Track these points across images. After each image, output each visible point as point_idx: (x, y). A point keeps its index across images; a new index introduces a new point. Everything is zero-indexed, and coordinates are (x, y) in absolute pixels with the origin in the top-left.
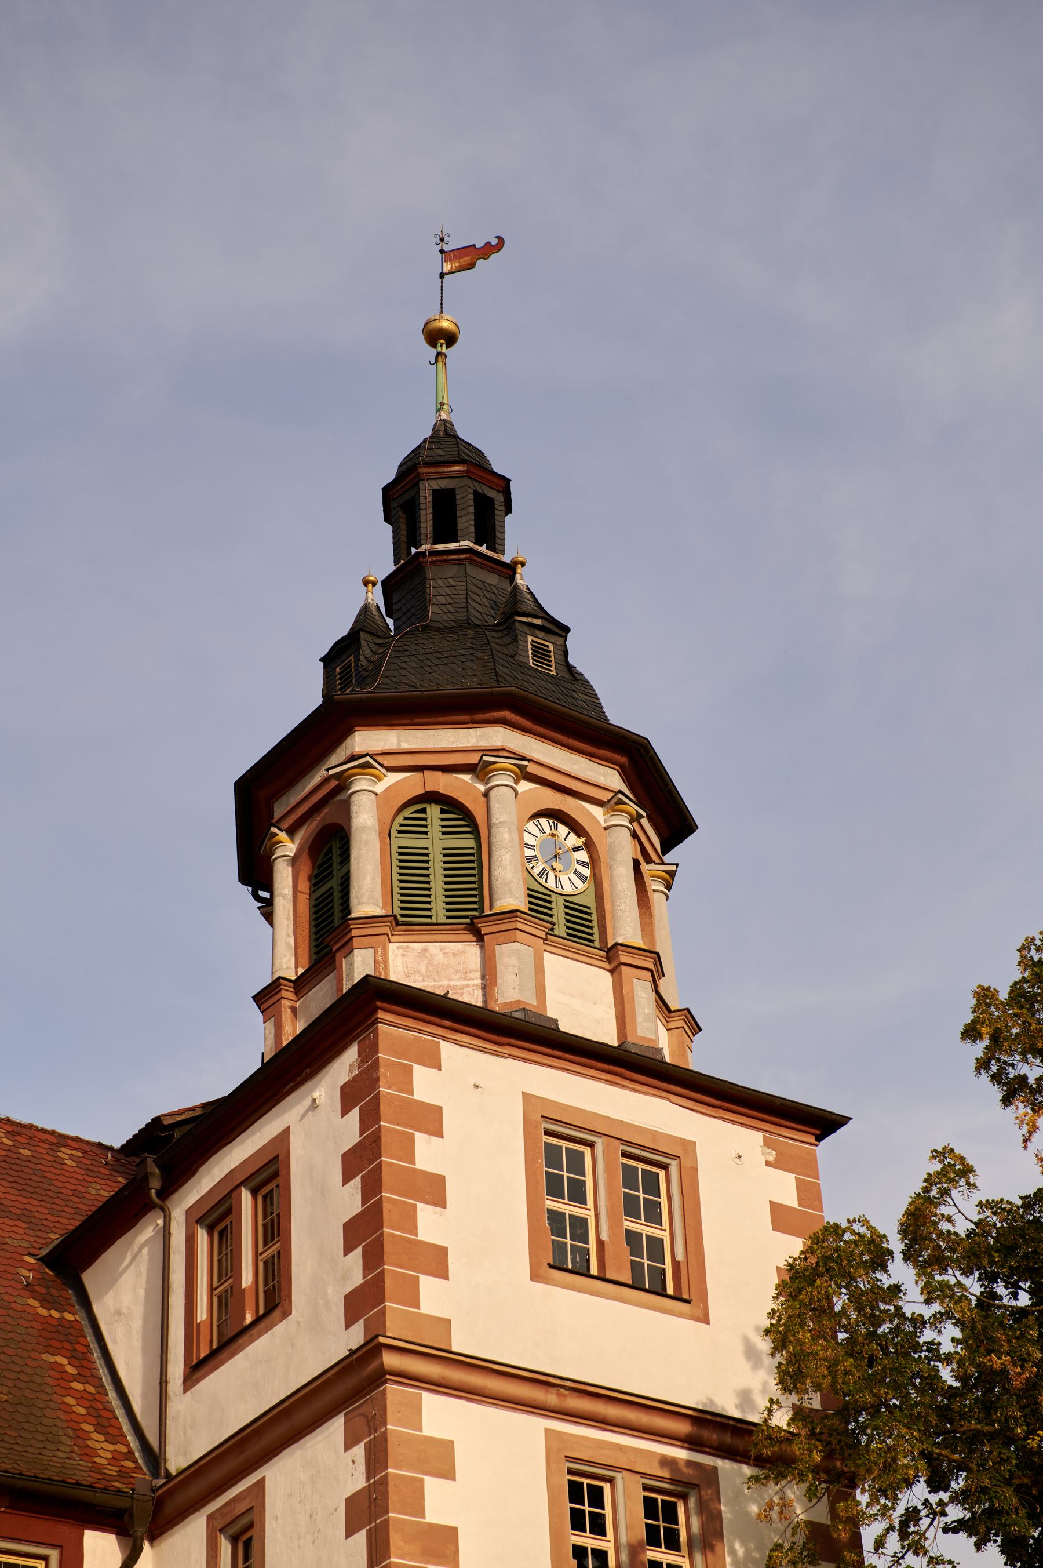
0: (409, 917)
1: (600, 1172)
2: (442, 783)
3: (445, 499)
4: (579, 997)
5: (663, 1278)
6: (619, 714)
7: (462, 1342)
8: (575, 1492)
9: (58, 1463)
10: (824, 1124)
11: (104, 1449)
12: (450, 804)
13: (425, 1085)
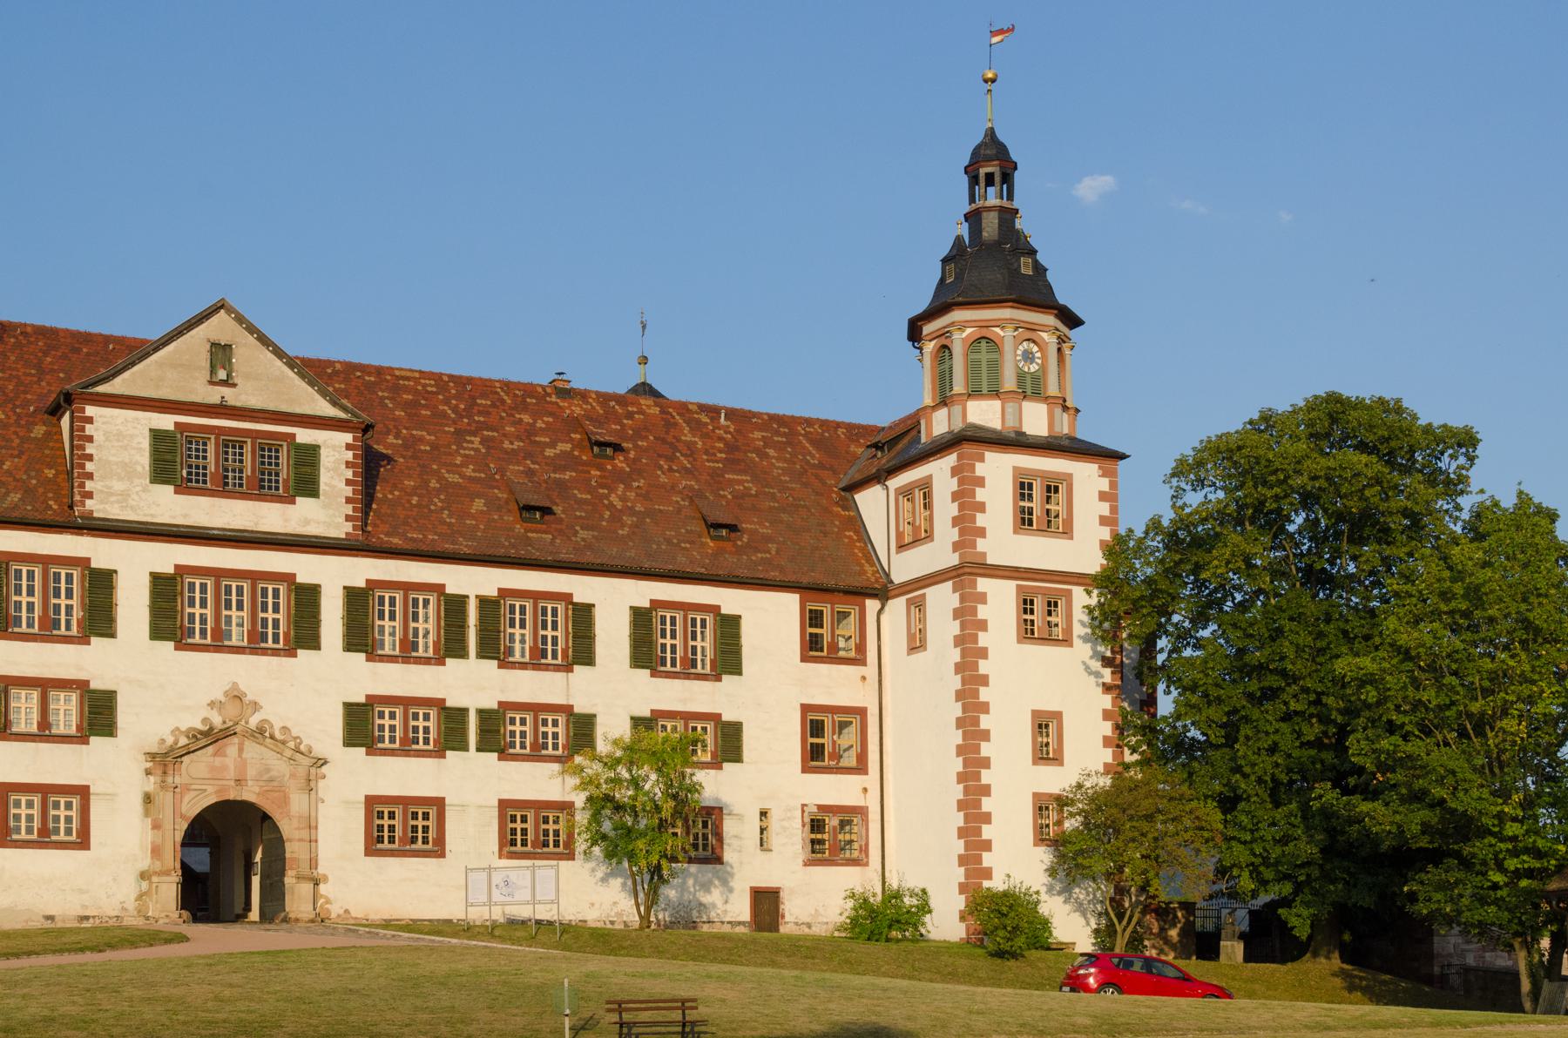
0: (975, 394)
1: (1038, 492)
2: (985, 332)
4: (1036, 420)
8: (1025, 602)
9: (856, 582)
10: (1122, 457)
12: (989, 340)
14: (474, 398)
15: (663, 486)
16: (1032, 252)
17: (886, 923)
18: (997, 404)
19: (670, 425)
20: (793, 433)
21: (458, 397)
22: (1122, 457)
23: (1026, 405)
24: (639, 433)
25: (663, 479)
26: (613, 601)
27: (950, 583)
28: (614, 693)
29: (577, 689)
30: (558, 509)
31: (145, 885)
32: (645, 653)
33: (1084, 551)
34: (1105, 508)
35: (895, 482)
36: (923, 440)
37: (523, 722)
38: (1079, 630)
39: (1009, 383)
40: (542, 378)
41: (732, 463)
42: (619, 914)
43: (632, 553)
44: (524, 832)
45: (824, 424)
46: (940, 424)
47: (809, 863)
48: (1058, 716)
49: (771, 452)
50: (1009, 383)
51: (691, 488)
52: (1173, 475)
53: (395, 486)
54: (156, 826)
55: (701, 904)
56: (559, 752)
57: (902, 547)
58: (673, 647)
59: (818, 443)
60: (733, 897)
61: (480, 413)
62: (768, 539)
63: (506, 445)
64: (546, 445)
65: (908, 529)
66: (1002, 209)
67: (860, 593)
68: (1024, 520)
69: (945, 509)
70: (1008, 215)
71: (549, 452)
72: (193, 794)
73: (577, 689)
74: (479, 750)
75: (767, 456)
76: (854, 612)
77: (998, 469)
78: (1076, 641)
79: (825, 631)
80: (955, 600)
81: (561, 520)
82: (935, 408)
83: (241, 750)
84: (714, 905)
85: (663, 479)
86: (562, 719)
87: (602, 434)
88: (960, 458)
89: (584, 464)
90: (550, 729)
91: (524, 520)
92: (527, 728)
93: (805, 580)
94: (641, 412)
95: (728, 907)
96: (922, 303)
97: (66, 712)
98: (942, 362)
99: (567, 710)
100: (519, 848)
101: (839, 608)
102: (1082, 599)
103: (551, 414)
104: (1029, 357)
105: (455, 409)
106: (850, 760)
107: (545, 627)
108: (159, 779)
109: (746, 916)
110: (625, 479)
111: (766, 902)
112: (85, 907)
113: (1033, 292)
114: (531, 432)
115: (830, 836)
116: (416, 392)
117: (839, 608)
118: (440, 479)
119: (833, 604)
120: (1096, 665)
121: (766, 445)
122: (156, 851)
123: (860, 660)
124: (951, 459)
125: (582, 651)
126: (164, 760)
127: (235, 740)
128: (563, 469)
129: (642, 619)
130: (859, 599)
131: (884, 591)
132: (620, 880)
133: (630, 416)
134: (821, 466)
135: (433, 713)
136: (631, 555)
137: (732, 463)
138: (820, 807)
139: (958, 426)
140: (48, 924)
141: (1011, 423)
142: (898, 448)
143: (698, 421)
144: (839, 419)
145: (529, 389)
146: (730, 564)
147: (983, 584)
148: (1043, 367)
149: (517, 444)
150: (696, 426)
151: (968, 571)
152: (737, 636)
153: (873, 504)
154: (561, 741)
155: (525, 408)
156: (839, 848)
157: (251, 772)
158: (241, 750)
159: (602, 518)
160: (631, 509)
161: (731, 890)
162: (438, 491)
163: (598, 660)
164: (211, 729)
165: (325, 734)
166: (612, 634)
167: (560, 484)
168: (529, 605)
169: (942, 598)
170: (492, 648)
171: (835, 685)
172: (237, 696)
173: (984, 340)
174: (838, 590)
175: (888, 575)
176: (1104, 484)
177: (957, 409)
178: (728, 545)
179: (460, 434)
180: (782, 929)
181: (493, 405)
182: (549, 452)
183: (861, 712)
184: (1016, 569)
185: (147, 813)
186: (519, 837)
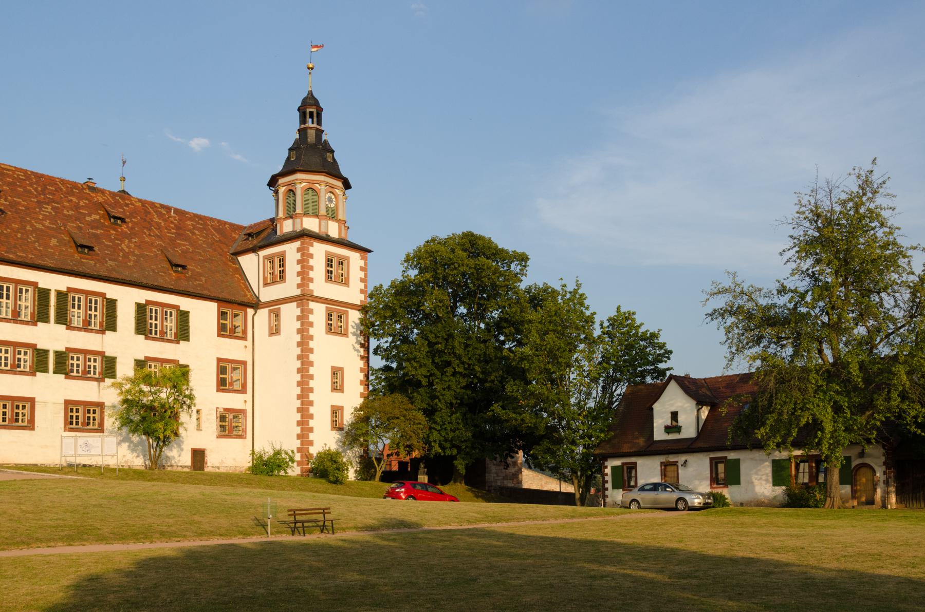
0: (306, 214)
1: (335, 263)
2: (311, 186)
3: (310, 109)
4: (333, 230)
5: (343, 281)
6: (344, 173)
7: (315, 294)
10: (370, 251)
11: (249, 294)
12: (313, 190)
13: (312, 250)
14: (45, 185)
15: (147, 242)
16: (332, 152)
17: (267, 467)
18: (317, 220)
19: (147, 213)
20: (205, 224)
21: (37, 183)
22: (370, 251)
23: (330, 222)
24: (132, 216)
25: (147, 239)
26: (128, 299)
27: (295, 304)
28: (126, 346)
29: (108, 343)
30: (96, 249)
32: (142, 327)
33: (353, 293)
34: (362, 274)
35: (264, 253)
36: (278, 233)
37: (78, 359)
38: (351, 330)
39: (323, 211)
40: (81, 180)
41: (179, 235)
42: (126, 462)
43: (135, 275)
44: (77, 417)
45: (219, 221)
46: (287, 227)
47: (219, 437)
48: (342, 369)
49: (197, 232)
50: (323, 211)
51: (161, 245)
52: (405, 261)
53: (7, 227)
55: (167, 457)
56: (97, 376)
57: (266, 284)
58: (156, 325)
59: (218, 230)
60: (183, 453)
61: (50, 194)
62: (200, 275)
63: (65, 212)
64: (85, 215)
65: (269, 276)
66: (317, 129)
67: (245, 305)
68: (329, 275)
69: (292, 268)
70: (319, 132)
71: (88, 219)
73: (108, 343)
74: (54, 373)
75: (195, 234)
76: (242, 314)
77: (319, 251)
78: (350, 335)
79: (228, 322)
80: (298, 312)
81: (98, 255)
82: (285, 219)
84: (174, 458)
85: (147, 239)
86: (99, 359)
87: (114, 212)
88: (302, 244)
89: (107, 227)
90: (92, 364)
91: (79, 252)
92: (80, 362)
93: (221, 297)
94: (132, 204)
95: (181, 458)
96: (279, 168)
98: (289, 197)
99: (102, 354)
100: (74, 426)
101: (236, 312)
102: (355, 317)
103: (87, 199)
104: (330, 200)
105: (36, 190)
106: (237, 386)
107: (90, 310)
109: (189, 463)
110: (129, 237)
111: (198, 456)
113: (333, 171)
114: (77, 207)
115: (230, 424)
116: (14, 178)
117: (236, 312)
118: (32, 226)
119: (363, 309)
120: (358, 346)
121: (194, 228)
123: (244, 338)
124: (297, 244)
125: (110, 324)
128: (97, 228)
129: (141, 309)
130: (244, 308)
131: (256, 305)
132: (127, 444)
133: (127, 205)
134: (220, 241)
135: (29, 352)
136: (136, 276)
137: (179, 235)
138: (225, 409)
139: (298, 229)
141: (323, 230)
142: (263, 236)
143: (161, 213)
144: (226, 220)
145: (74, 185)
146: (183, 285)
147: (312, 305)
148: (336, 205)
149: (71, 213)
150: (160, 215)
151: (304, 298)
152: (187, 322)
153: (250, 264)
154: (97, 371)
155: (73, 194)
156: (231, 431)
159: (118, 255)
160: (133, 252)
161: (182, 450)
162: (32, 232)
163: (118, 328)
166: (126, 316)
167: (95, 235)
168: (83, 298)
169: (290, 312)
170: (62, 318)
171: (233, 349)
173: (311, 189)
174: (235, 302)
175: (258, 298)
176: (362, 263)
177: (298, 221)
178: (182, 276)
179: (40, 203)
180: (206, 470)
181: (56, 190)
182: (88, 219)
183: (244, 363)
184: (326, 299)
186: (74, 420)
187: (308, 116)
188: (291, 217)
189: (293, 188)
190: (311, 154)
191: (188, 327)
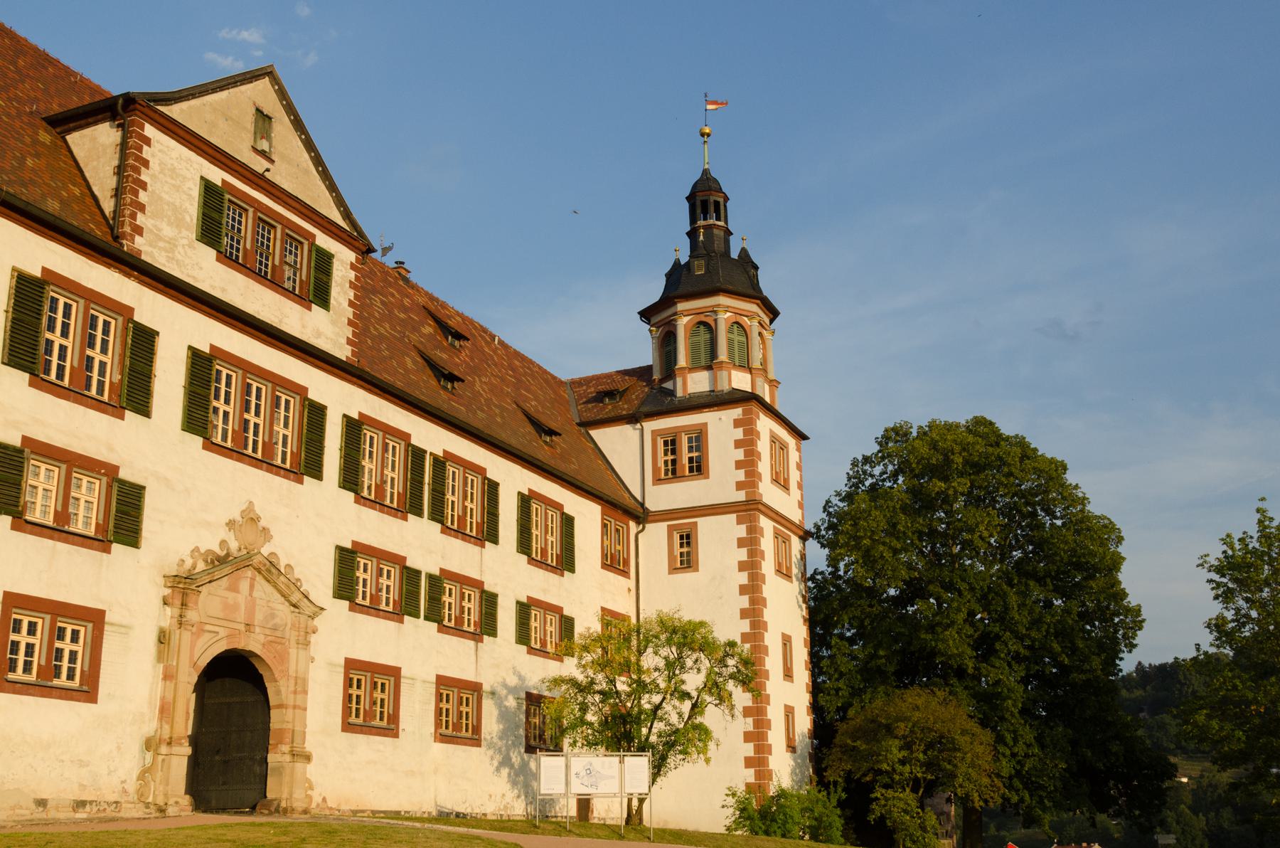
2: (739, 319)
31: (149, 756)
35: (651, 426)
46: (697, 383)
54: (168, 676)
72: (207, 636)
82: (693, 369)
83: (252, 587)
97: (89, 504)
108: (177, 612)
112: (83, 787)
122: (165, 711)
126: (183, 587)
127: (249, 573)
140: (39, 814)
157: (259, 617)
158: (252, 587)
164: (228, 555)
165: (318, 578)
172: (251, 518)
185: (160, 657)
187: (712, 208)
188: (709, 368)
189: (710, 321)
190: (713, 266)
191: (573, 545)
